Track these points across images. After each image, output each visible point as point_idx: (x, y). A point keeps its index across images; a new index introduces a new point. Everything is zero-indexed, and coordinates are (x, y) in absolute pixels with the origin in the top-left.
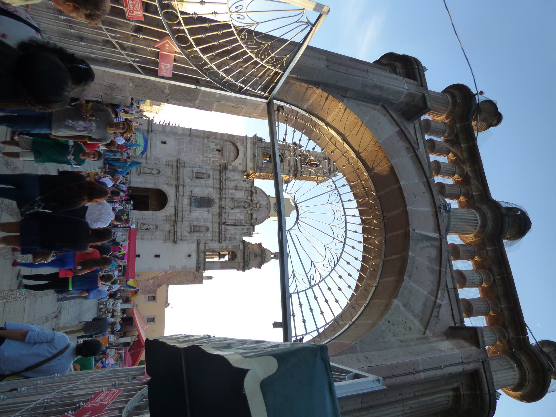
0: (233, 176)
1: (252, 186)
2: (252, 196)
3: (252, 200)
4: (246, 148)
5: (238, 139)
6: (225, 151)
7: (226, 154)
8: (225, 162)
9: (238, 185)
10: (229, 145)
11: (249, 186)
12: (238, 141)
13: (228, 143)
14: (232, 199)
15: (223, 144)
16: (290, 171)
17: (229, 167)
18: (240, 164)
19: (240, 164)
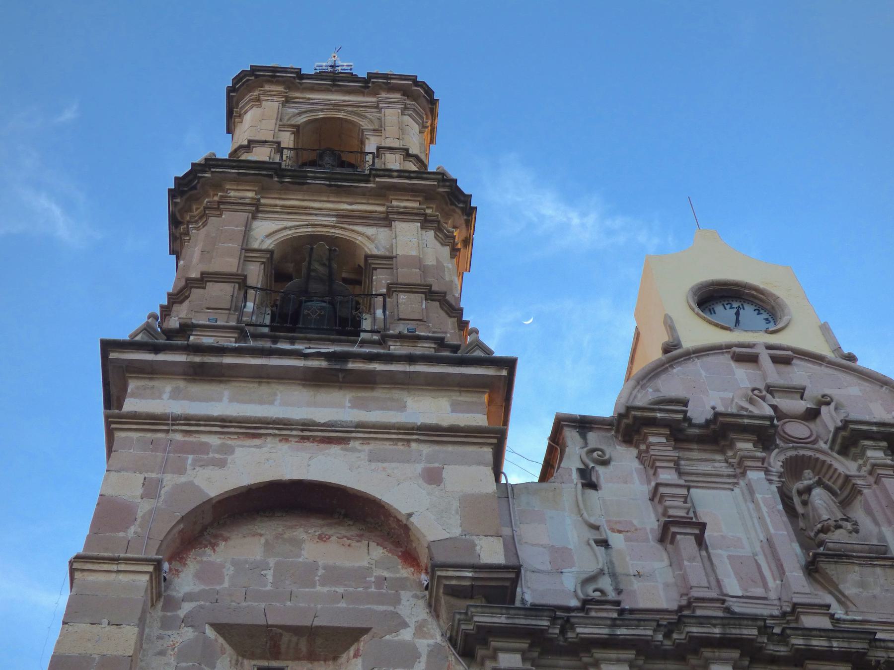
0: (560, 556)
1: (631, 426)
2: (719, 433)
3: (765, 435)
4: (253, 429)
5: (151, 489)
6: (283, 614)
7: (322, 605)
8: (413, 608)
9: (649, 521)
10: (210, 574)
11: (625, 458)
12: (170, 480)
13: (186, 581)
14: (812, 569)
15: (188, 621)
16: (426, 222)
17: (491, 552)
18: (433, 477)
19: (433, 477)
